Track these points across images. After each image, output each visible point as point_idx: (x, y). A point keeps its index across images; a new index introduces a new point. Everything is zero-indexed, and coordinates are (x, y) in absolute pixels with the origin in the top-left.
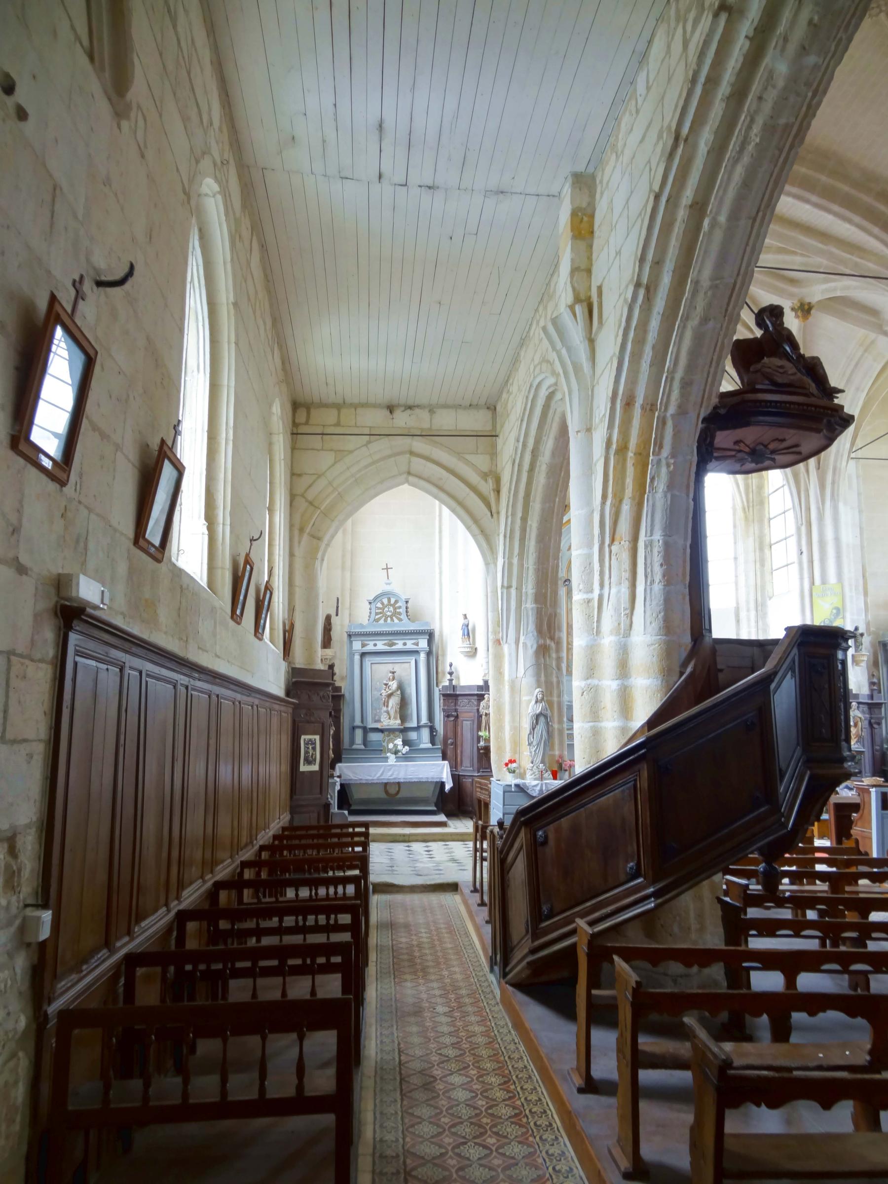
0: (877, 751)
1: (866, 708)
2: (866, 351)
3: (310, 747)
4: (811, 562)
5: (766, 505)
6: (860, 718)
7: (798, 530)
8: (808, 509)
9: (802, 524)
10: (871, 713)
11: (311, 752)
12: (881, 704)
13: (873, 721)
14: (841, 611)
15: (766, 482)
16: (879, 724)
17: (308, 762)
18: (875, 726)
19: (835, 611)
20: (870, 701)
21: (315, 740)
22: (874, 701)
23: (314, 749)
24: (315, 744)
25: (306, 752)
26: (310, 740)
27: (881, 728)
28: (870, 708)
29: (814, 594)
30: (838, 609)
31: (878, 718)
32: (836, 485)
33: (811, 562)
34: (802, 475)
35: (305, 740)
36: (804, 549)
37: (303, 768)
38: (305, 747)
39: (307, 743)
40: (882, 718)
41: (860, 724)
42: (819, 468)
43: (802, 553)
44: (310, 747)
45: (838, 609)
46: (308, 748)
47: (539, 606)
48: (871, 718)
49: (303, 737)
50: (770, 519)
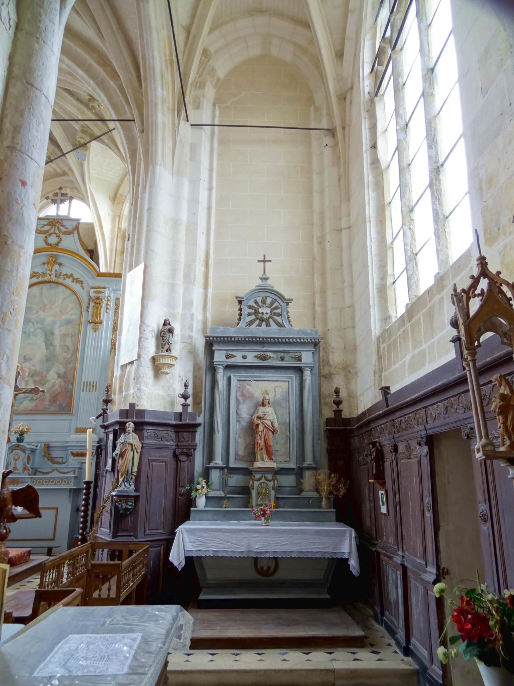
0: (181, 495)
1: (171, 433)
6: (132, 445)
10: (178, 439)
13: (179, 451)
16: (189, 455)
18: (182, 458)
20: (178, 422)
22: (182, 422)
27: (192, 462)
28: (177, 432)
31: (188, 447)
40: (194, 448)
41: (129, 454)
42: (143, 131)
48: (177, 446)
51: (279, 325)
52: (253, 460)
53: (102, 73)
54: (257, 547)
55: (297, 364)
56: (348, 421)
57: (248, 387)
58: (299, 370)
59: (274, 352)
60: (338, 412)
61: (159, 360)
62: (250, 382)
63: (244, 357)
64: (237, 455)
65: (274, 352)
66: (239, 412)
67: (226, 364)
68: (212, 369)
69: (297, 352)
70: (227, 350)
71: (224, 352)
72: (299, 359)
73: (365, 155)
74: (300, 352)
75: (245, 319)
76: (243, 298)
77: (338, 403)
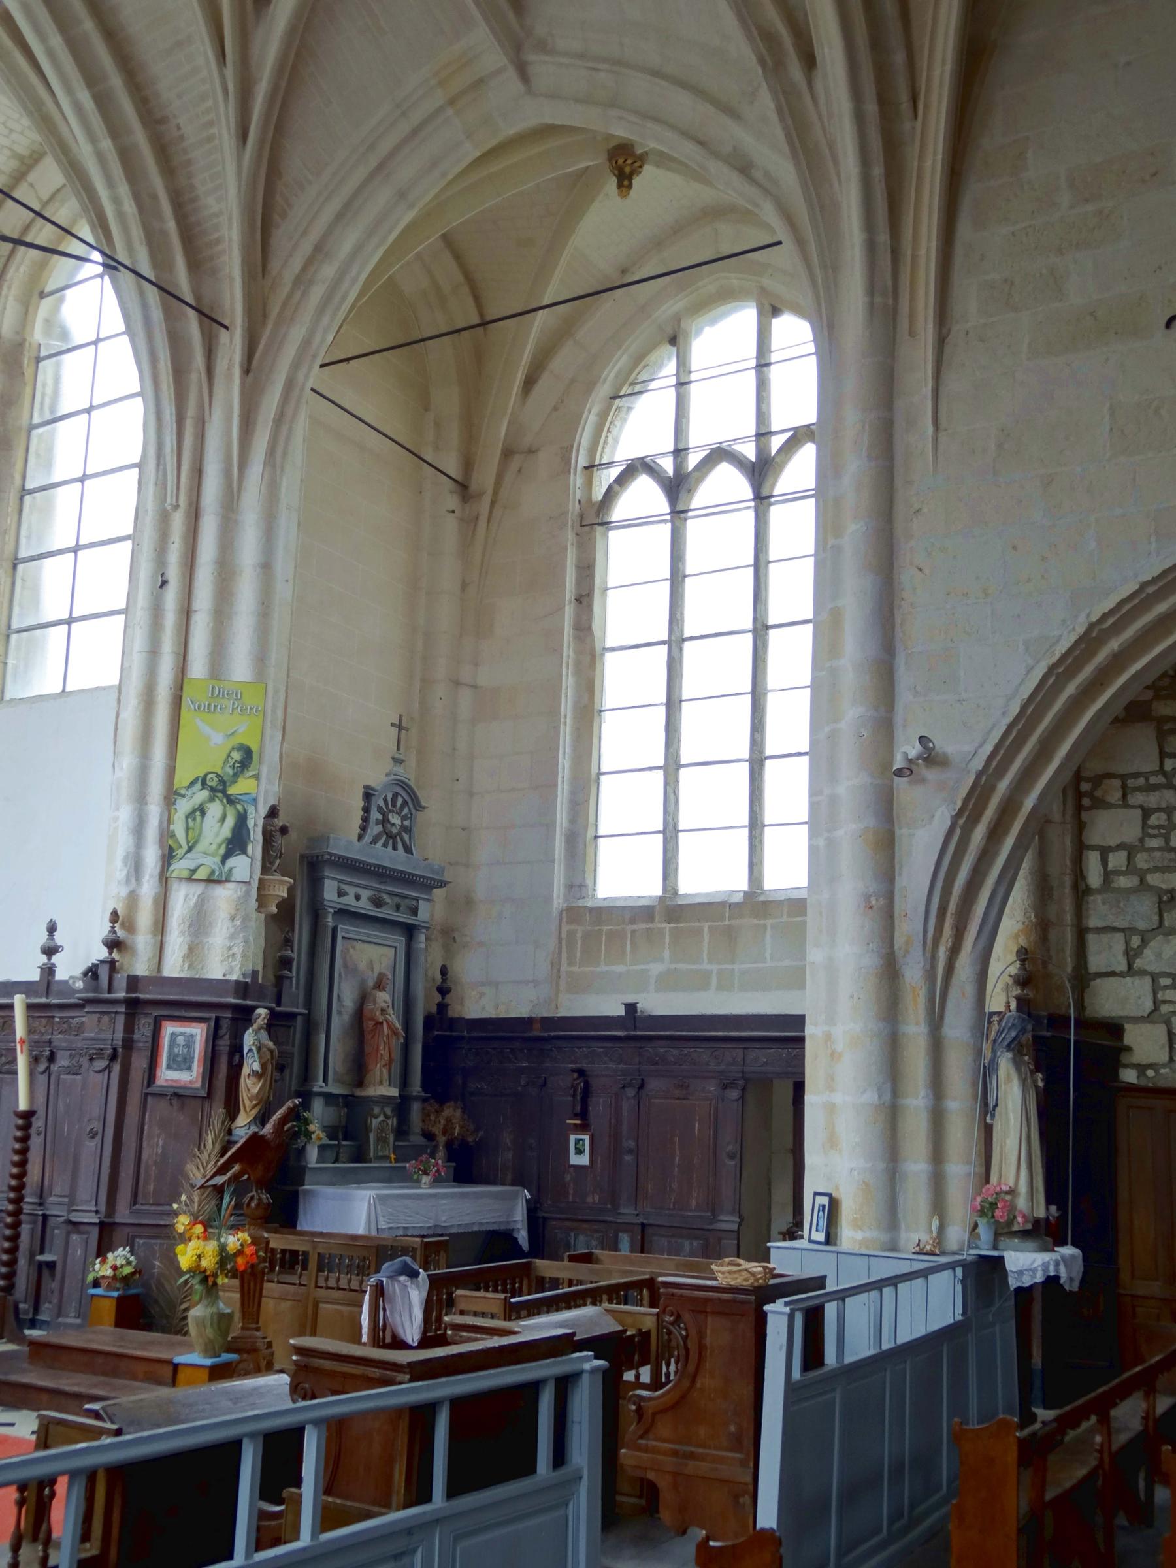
2: (452, 102)
4: (186, 612)
5: (20, 453)
7: (164, 519)
8: (198, 472)
9: (177, 507)
12: (292, 1016)
14: (255, 757)
15: (28, 390)
19: (237, 756)
29: (186, 701)
30: (247, 753)
32: (284, 429)
33: (186, 612)
34: (194, 377)
36: (174, 573)
43: (164, 583)
45: (247, 753)
50: (24, 492)
51: (408, 850)
52: (360, 1083)
53: (140, 137)
54: (444, 1219)
55: (410, 920)
56: (454, 1023)
57: (351, 950)
58: (410, 931)
59: (391, 894)
60: (442, 1007)
61: (271, 888)
62: (355, 943)
63: (358, 898)
64: (335, 1072)
65: (391, 894)
66: (341, 995)
67: (339, 906)
68: (316, 911)
69: (413, 898)
70: (340, 881)
71: (336, 883)
72: (414, 911)
73: (567, 608)
74: (417, 899)
75: (372, 830)
76: (376, 791)
77: (443, 991)
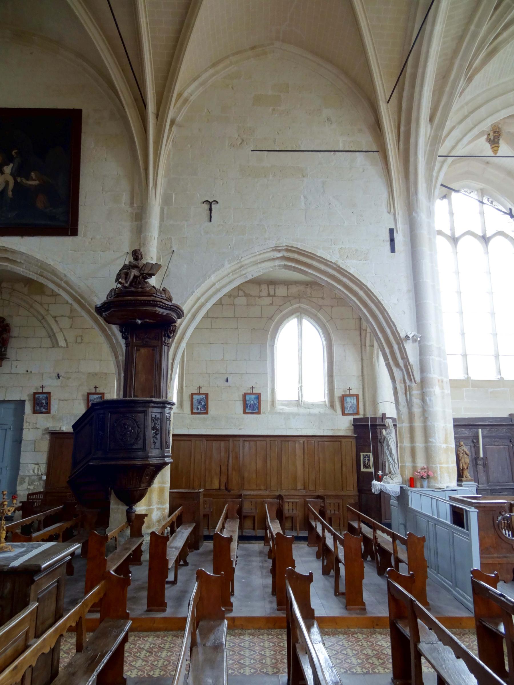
3: (367, 459)
11: (367, 461)
17: (367, 466)
21: (370, 455)
23: (369, 460)
24: (369, 457)
25: (364, 462)
26: (367, 455)
35: (363, 455)
37: (363, 470)
38: (363, 459)
39: (364, 457)
44: (367, 459)
46: (366, 459)
47: (387, 362)
49: (362, 454)
